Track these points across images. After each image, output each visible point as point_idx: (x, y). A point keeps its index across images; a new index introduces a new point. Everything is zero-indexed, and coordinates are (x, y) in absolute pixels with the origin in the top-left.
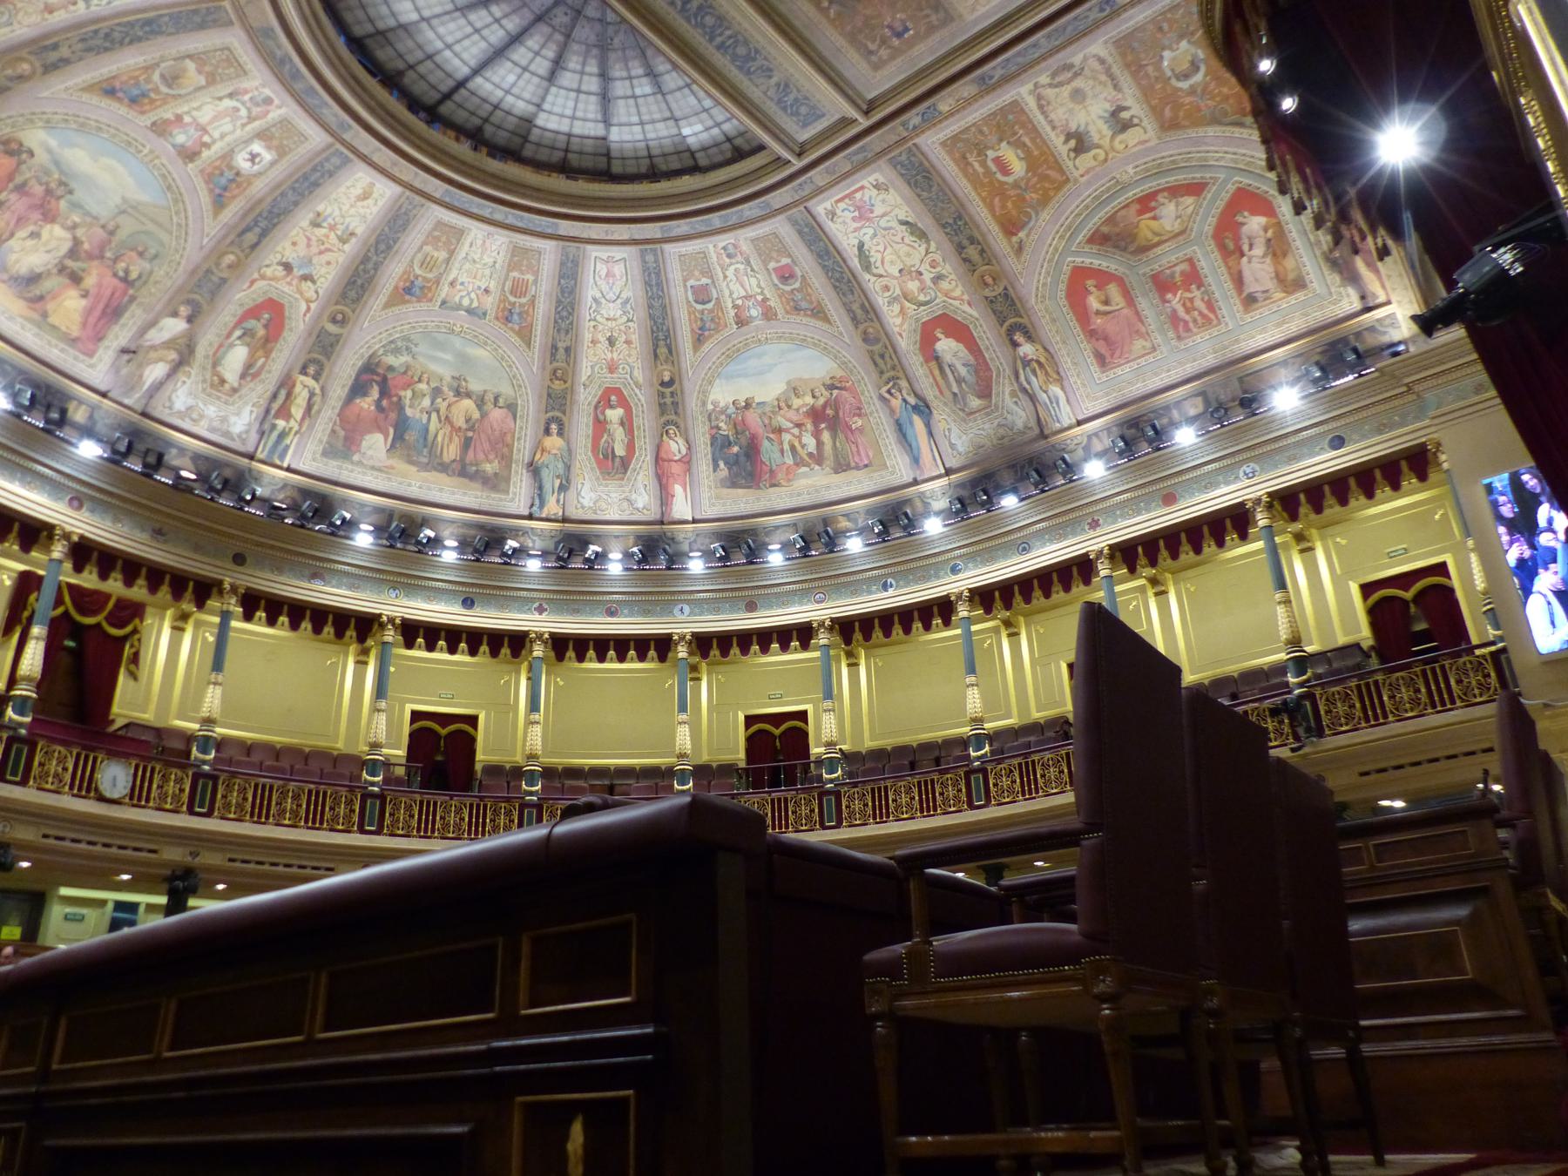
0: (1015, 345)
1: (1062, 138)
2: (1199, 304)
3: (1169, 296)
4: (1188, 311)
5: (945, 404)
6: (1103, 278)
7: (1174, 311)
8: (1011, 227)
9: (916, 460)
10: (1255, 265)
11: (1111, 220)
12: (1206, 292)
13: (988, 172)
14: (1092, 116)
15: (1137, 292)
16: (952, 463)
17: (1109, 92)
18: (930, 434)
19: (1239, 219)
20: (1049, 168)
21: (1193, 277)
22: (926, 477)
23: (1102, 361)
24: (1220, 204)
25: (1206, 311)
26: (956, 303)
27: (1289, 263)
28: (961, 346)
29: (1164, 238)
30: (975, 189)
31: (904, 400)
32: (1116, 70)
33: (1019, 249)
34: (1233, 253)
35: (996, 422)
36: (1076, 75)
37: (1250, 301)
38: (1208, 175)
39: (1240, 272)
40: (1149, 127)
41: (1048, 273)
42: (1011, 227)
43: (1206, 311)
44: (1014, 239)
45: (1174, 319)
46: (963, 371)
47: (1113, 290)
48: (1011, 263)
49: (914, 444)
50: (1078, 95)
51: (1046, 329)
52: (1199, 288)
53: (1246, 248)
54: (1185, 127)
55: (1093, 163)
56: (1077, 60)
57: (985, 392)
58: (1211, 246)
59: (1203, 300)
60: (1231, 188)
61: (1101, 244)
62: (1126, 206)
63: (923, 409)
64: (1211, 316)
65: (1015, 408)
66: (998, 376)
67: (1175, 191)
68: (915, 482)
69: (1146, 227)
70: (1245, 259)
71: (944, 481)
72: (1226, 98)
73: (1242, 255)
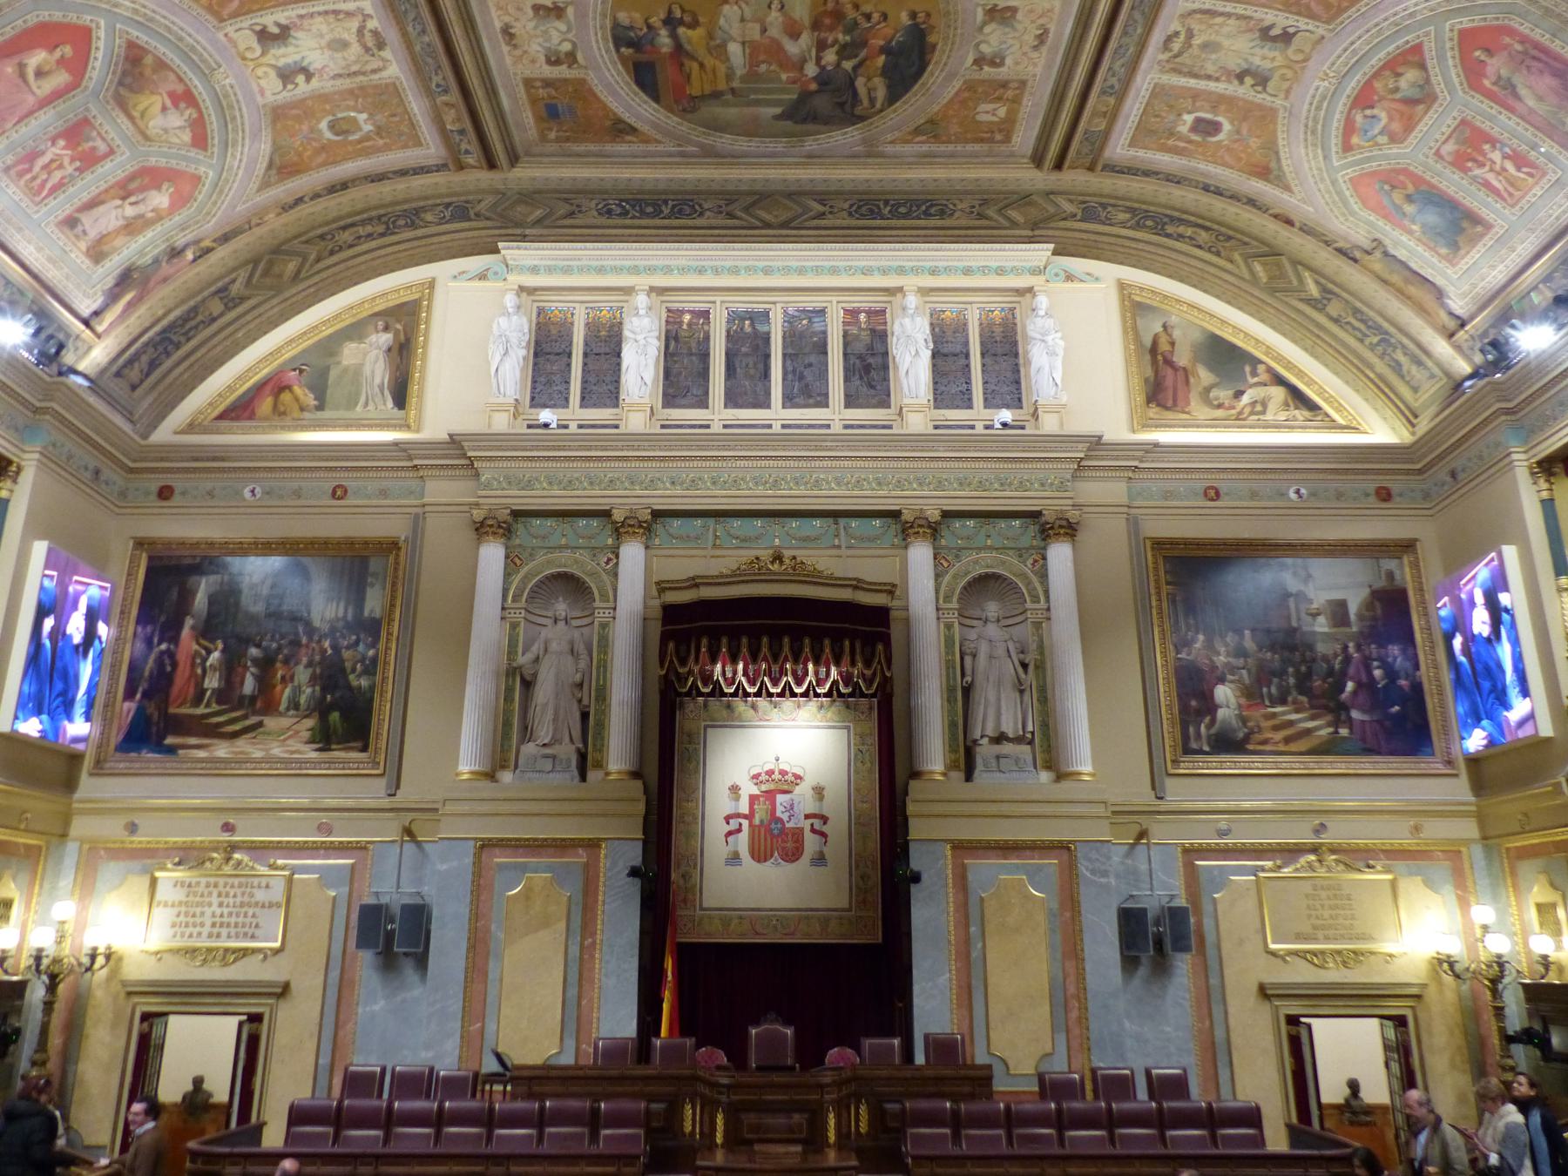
1: (283, 21)
2: (57, 176)
4: (45, 167)
6: (78, 66)
7: (43, 153)
11: (161, 65)
14: (307, 48)
15: (61, 106)
21: (89, 161)
25: (49, 185)
29: (138, 121)
32: (361, 78)
37: (71, 222)
38: (216, 150)
39: (102, 202)
40: (279, 97)
43: (49, 185)
45: (32, 157)
47: (61, 78)
52: (76, 169)
53: (133, 199)
59: (62, 178)
61: (127, 58)
62: (181, 80)
64: (44, 194)
69: (151, 103)
70: (119, 202)
73: (124, 198)
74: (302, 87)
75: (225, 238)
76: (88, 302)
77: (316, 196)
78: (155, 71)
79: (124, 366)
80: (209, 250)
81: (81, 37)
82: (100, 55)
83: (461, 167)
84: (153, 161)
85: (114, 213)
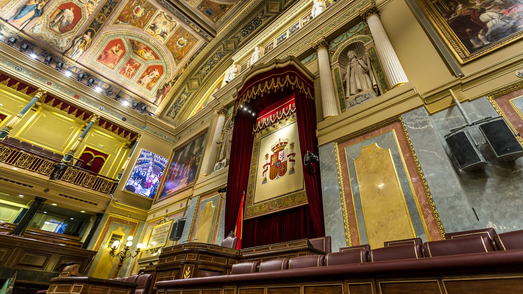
0: (86, 33)
1: (153, 23)
2: (131, 72)
3: (129, 65)
4: (128, 71)
5: (48, 20)
6: (122, 47)
7: (126, 68)
8: (121, 18)
9: (15, 18)
10: (148, 78)
11: (139, 43)
12: (135, 72)
13: (134, 8)
14: (161, 28)
15: (124, 57)
16: (26, 30)
17: (169, 30)
18: (31, 19)
19: (156, 69)
20: (143, 23)
21: (137, 68)
22: (12, 24)
23: (100, 58)
24: (156, 64)
25: (131, 75)
26: (87, 11)
27: (153, 84)
28: (73, 18)
29: (142, 56)
30: (127, 5)
31: (37, 6)
32: (175, 29)
33: (116, 23)
34: (147, 72)
35: (55, 38)
36: (170, 21)
37: (140, 82)
38: (161, 58)
39: (144, 76)
40: (165, 41)
41: (114, 33)
42: (121, 18)
43: (131, 75)
44: (118, 21)
45: (124, 69)
46: (64, 21)
47: (121, 52)
48: (111, 22)
49: (22, 15)
50: (165, 23)
51: (98, 40)
52: (135, 70)
53: (150, 74)
54: (169, 49)
55: (150, 33)
56: (174, 20)
57: (63, 30)
58: (146, 67)
59: (133, 72)
60: (161, 64)
61: (131, 43)
62: (144, 45)
63: (39, 13)
64: (131, 76)
65: (65, 42)
66: (72, 32)
67: (154, 53)
68: (6, 21)
69: (142, 51)
70: (148, 75)
71: (17, 31)
72: (179, 54)
73: (149, 74)
74: (168, 37)
75: (176, 79)
76: (152, 99)
77: (189, 63)
78: (138, 45)
79: (168, 113)
80: (174, 83)
81: (120, 41)
82: (126, 44)
83: (210, 42)
84: (150, 65)
85: (148, 78)
